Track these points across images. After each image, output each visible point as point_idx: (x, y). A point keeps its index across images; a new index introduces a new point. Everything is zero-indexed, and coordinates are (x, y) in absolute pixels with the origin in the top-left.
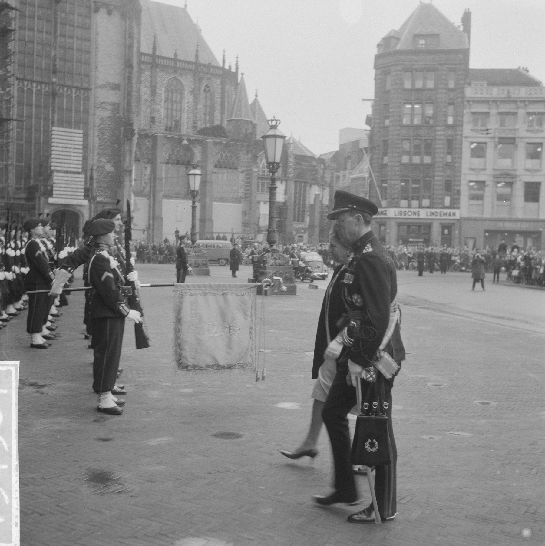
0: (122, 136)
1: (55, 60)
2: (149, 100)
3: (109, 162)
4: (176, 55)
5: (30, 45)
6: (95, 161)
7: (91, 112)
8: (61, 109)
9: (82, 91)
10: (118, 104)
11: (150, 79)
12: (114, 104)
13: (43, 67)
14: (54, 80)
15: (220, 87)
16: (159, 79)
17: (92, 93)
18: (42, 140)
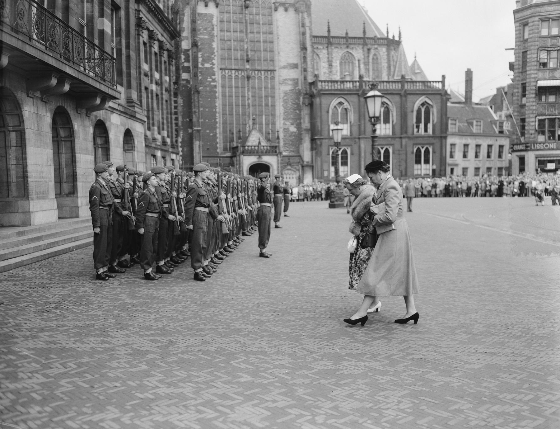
0: (301, 103)
1: (247, 52)
2: (327, 72)
3: (292, 124)
4: (347, 34)
5: (229, 43)
6: (282, 125)
8: (254, 88)
9: (269, 73)
10: (297, 79)
11: (327, 56)
12: (294, 80)
13: (239, 58)
14: (248, 67)
15: (386, 53)
16: (334, 55)
17: (277, 74)
18: (241, 113)
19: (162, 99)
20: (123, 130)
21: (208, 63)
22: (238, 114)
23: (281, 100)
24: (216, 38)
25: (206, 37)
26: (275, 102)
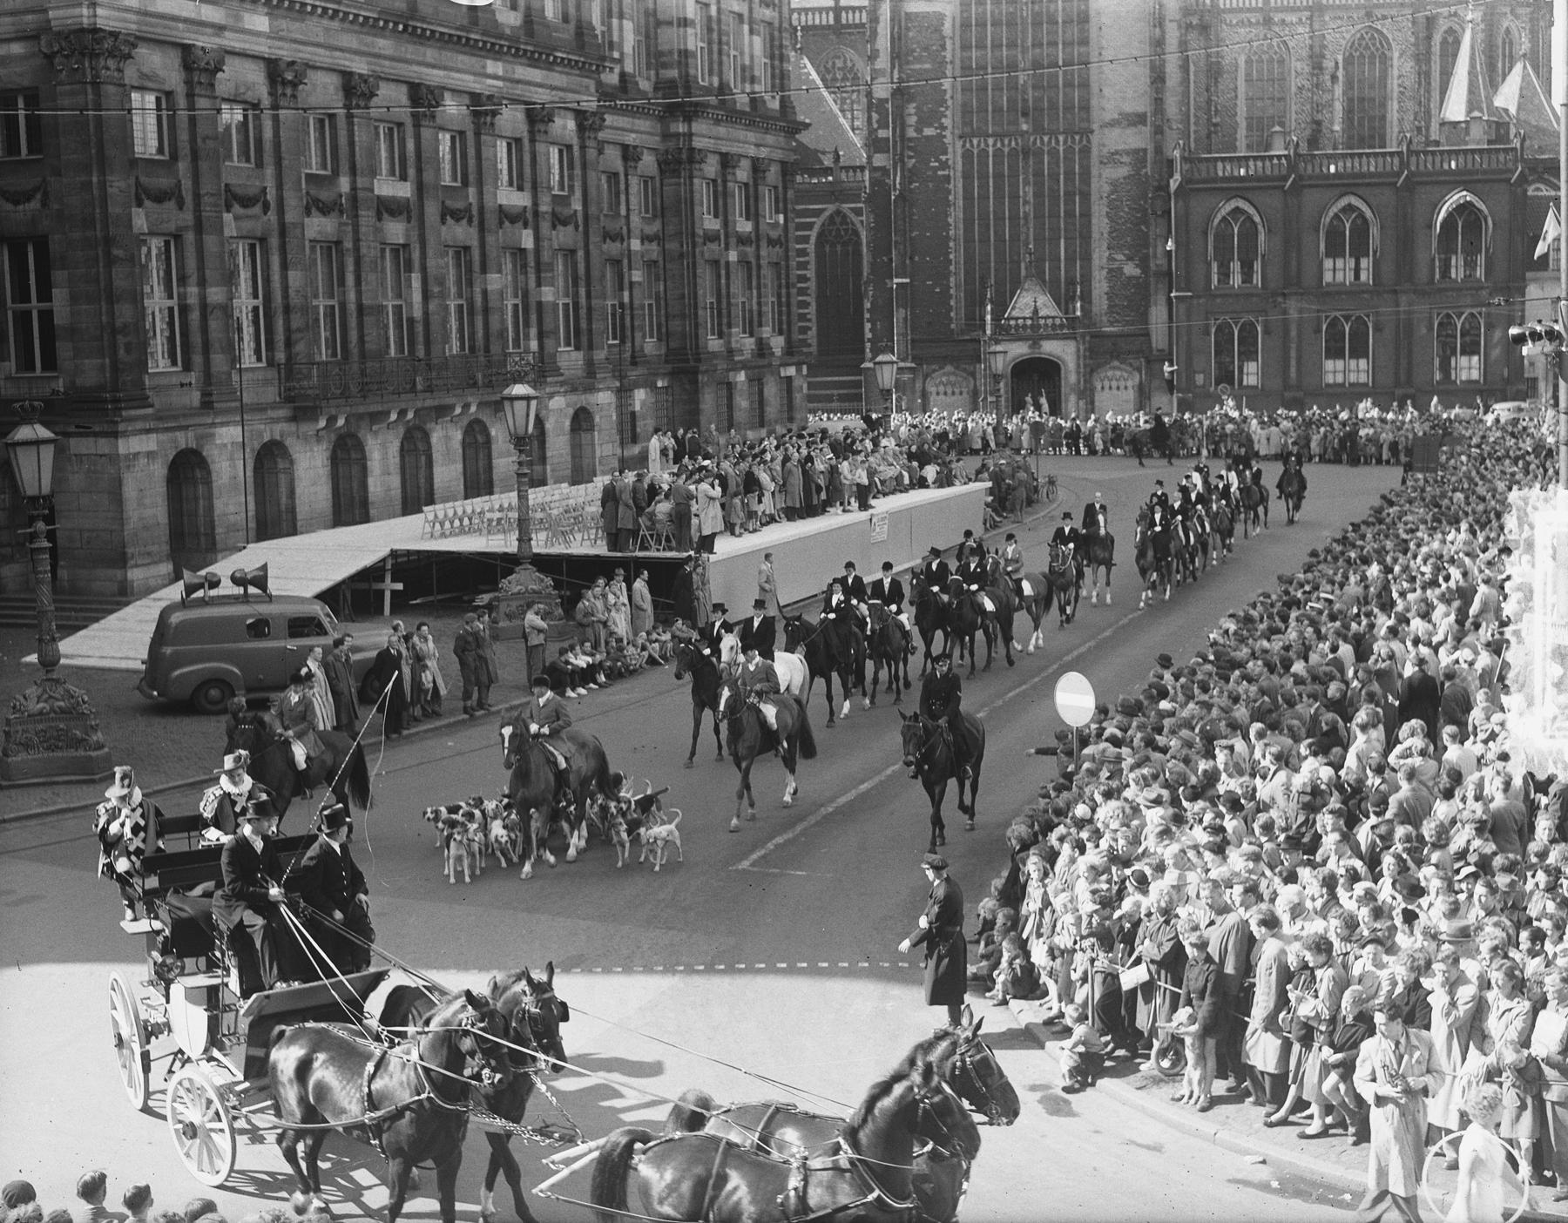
1: (1025, 92)
2: (1307, 84)
3: (1130, 259)
7: (1094, 172)
8: (1038, 174)
10: (1145, 150)
12: (1136, 151)
14: (1025, 127)
17: (1095, 139)
19: (759, 267)
20: (571, 411)
21: (930, 125)
22: (1000, 238)
23: (1105, 201)
24: (949, 67)
25: (927, 66)
26: (1089, 208)
